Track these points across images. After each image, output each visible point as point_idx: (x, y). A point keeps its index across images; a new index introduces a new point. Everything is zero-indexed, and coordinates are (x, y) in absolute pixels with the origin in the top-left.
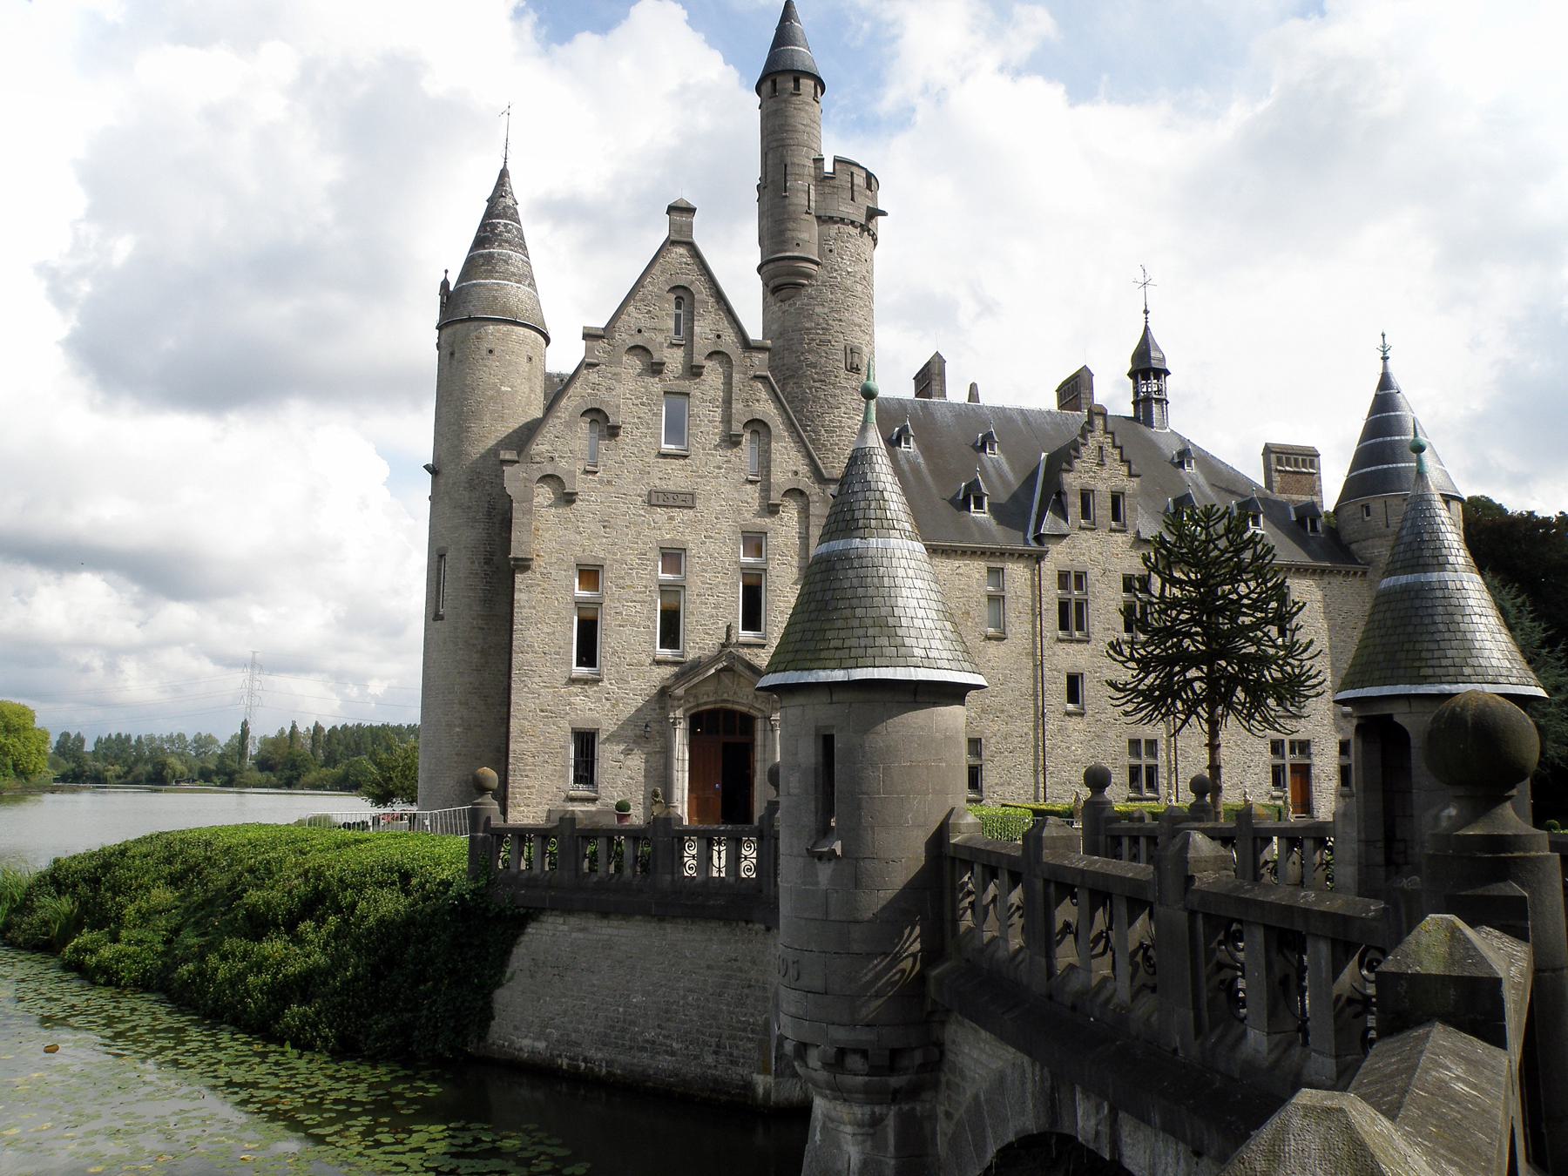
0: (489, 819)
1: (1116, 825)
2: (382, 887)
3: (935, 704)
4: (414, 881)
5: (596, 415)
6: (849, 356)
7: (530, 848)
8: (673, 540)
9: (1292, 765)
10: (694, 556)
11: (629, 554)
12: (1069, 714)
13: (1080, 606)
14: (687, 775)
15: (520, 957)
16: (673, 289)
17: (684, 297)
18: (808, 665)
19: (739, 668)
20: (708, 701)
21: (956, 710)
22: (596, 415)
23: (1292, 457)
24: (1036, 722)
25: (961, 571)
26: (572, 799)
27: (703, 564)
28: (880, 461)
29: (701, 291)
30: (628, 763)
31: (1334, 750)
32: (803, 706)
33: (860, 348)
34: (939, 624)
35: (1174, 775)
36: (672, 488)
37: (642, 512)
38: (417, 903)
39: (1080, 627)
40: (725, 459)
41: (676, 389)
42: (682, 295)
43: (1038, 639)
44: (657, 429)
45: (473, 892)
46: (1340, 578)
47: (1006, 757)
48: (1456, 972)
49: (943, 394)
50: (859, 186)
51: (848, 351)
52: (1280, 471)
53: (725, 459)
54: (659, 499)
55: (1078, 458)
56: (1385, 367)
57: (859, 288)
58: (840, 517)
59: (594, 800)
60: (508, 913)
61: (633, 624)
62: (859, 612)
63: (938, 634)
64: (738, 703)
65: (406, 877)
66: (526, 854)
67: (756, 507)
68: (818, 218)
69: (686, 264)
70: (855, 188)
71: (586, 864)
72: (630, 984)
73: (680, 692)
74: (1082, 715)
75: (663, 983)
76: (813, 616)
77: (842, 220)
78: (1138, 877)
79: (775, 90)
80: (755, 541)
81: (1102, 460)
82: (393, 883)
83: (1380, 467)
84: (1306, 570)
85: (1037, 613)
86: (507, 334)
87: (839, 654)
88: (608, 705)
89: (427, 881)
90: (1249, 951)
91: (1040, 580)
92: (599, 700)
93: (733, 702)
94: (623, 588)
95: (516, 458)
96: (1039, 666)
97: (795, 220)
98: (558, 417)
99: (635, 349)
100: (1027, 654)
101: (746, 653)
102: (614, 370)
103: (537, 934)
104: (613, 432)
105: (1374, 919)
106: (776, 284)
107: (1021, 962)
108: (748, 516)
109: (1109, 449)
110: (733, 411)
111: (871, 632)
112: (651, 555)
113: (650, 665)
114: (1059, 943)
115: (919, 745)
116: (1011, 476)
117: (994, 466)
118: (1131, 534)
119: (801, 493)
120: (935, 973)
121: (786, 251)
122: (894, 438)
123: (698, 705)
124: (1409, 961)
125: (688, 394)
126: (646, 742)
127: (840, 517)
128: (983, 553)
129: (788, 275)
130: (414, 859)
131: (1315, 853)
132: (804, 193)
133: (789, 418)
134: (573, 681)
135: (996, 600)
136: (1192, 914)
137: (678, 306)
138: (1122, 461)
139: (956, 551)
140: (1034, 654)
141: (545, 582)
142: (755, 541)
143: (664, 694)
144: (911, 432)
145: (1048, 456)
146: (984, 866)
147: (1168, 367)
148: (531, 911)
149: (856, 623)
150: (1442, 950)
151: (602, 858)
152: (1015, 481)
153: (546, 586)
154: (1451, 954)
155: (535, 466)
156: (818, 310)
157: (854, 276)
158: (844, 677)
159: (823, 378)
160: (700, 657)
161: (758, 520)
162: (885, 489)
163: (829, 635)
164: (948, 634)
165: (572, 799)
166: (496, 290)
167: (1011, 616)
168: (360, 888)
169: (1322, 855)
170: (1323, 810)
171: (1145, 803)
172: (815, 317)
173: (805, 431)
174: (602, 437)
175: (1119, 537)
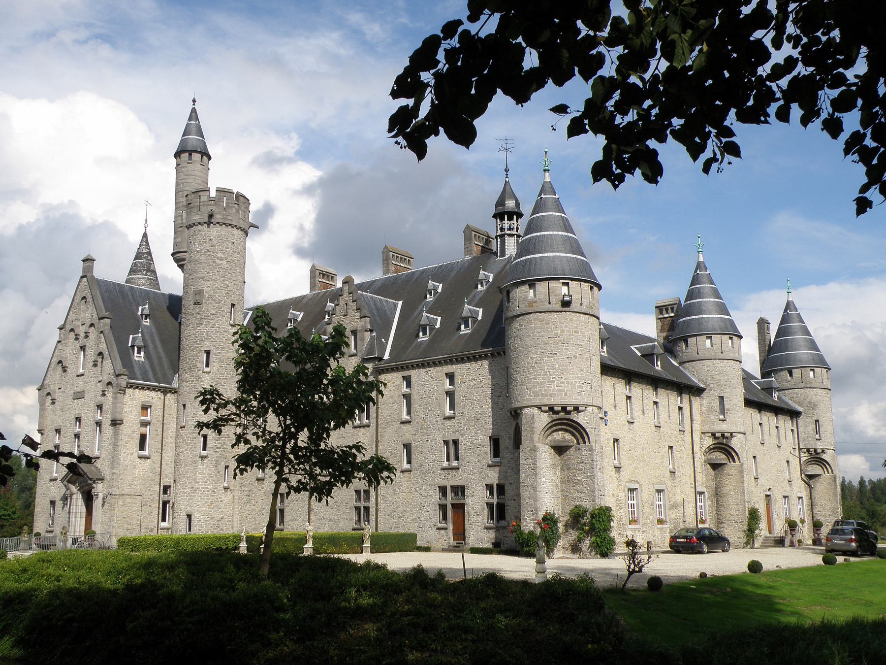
47: (295, 504)
59: (52, 532)
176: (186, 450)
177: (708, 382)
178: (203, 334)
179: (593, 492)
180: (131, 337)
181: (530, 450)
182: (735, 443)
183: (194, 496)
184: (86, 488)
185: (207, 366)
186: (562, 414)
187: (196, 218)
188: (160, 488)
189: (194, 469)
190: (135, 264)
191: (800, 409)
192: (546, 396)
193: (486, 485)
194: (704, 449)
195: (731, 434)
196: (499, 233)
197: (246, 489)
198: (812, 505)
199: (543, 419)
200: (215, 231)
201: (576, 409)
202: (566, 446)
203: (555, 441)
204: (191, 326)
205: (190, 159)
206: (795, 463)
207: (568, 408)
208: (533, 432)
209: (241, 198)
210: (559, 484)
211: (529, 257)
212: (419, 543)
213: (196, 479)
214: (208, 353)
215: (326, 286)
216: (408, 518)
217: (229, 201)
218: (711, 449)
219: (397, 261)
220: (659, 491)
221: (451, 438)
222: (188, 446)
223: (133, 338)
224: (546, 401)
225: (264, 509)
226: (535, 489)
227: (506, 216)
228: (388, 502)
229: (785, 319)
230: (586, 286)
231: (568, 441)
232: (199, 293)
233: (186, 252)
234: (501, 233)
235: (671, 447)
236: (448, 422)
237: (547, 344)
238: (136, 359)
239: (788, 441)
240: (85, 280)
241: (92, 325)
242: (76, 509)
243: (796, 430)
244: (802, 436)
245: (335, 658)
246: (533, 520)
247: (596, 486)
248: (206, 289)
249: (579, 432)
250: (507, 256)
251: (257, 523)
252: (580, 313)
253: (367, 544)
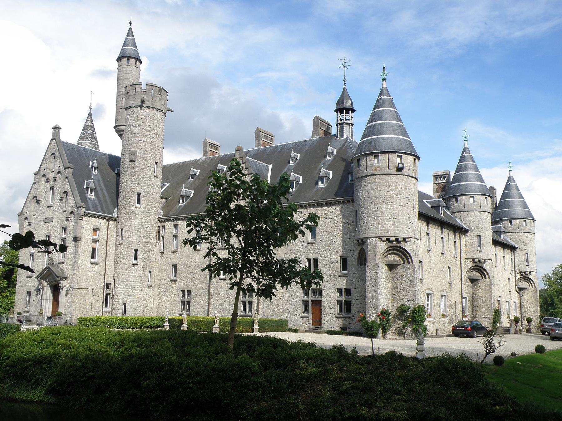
9: (312, 301)
59: (28, 312)
102: (39, 183)
157: (135, 126)
176: (123, 260)
177: (471, 226)
178: (136, 182)
179: (414, 295)
180: (86, 181)
181: (373, 266)
182: (487, 266)
183: (128, 290)
184: (53, 283)
185: (138, 203)
186: (395, 243)
187: (132, 103)
188: (104, 284)
189: (129, 272)
190: (83, 133)
191: (516, 246)
192: (385, 230)
193: (337, 289)
194: (467, 269)
195: (485, 260)
196: (339, 122)
197: (163, 287)
198: (521, 307)
199: (382, 246)
200: (145, 112)
201: (405, 240)
202: (396, 265)
203: (388, 261)
204: (128, 176)
205: (128, 62)
206: (513, 280)
207: (400, 239)
208: (376, 255)
209: (163, 91)
210: (390, 290)
211: (374, 137)
212: (289, 326)
213: (129, 279)
214: (139, 194)
215: (213, 153)
216: (280, 309)
217: (155, 93)
218: (471, 270)
219: (264, 139)
220: (443, 296)
221: (312, 257)
222: (124, 256)
223: (87, 182)
224: (385, 234)
225: (175, 300)
226: (376, 293)
227: (344, 111)
229: (507, 187)
230: (412, 158)
231: (397, 261)
232: (134, 153)
233: (125, 125)
234: (341, 122)
235: (449, 268)
236: (310, 246)
237: (386, 196)
238: (90, 197)
239: (509, 266)
240: (54, 141)
241: (59, 172)
242: (46, 297)
243: (513, 259)
244: (517, 263)
245: (304, 411)
246: (375, 313)
247: (416, 292)
248: (138, 151)
249: (405, 255)
250: (344, 138)
251: (170, 309)
252: (408, 176)
253: (256, 326)
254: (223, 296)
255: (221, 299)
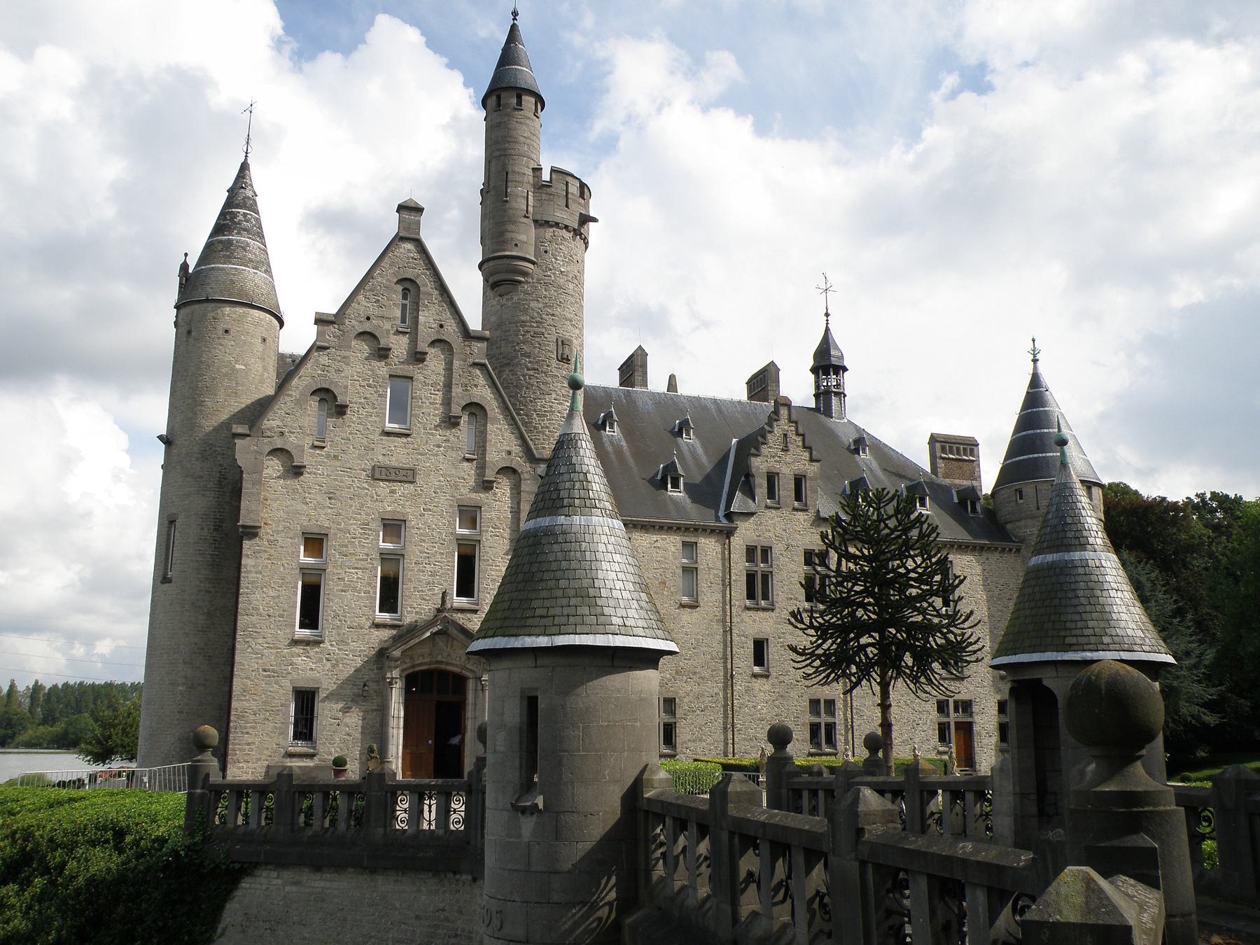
0: (207, 775)
1: (797, 780)
2: (94, 846)
3: (631, 669)
4: (128, 839)
5: (325, 395)
6: (560, 348)
7: (247, 803)
8: (394, 512)
9: (957, 723)
10: (413, 527)
11: (352, 524)
12: (755, 676)
13: (766, 577)
14: (401, 731)
15: (232, 912)
16: (400, 281)
17: (410, 288)
18: (515, 631)
19: (453, 631)
20: (423, 661)
21: (650, 673)
22: (325, 395)
23: (955, 446)
24: (725, 683)
25: (658, 544)
26: (291, 755)
27: (421, 535)
28: (584, 446)
29: (427, 284)
30: (347, 720)
31: (994, 710)
32: (510, 669)
33: (571, 341)
34: (635, 595)
35: (850, 732)
36: (395, 464)
37: (365, 485)
38: (130, 861)
39: (765, 597)
40: (445, 438)
41: (401, 373)
42: (409, 286)
43: (728, 607)
44: (382, 409)
45: (188, 848)
46: (997, 555)
47: (698, 715)
48: (1092, 920)
49: (645, 384)
50: (572, 194)
51: (560, 343)
52: (944, 458)
53: (445, 438)
54: (381, 474)
55: (765, 444)
56: (1035, 368)
57: (571, 286)
58: (547, 496)
59: (311, 756)
60: (223, 867)
61: (355, 589)
62: (563, 583)
63: (635, 604)
64: (452, 664)
65: (120, 834)
66: (243, 809)
67: (472, 483)
68: (536, 222)
69: (413, 258)
70: (569, 196)
71: (302, 818)
72: (340, 936)
73: (397, 653)
74: (767, 677)
75: (373, 934)
76: (521, 586)
77: (557, 225)
78: (814, 830)
79: (499, 104)
80: (470, 515)
81: (787, 447)
82: (107, 841)
83: (1031, 456)
84: (967, 547)
85: (726, 584)
86: (244, 315)
87: (544, 621)
88: (328, 665)
89: (141, 838)
90: (915, 898)
91: (730, 554)
92: (320, 660)
93: (447, 664)
94: (346, 556)
95: (248, 432)
96: (728, 632)
97: (514, 223)
98: (289, 395)
99: (362, 335)
100: (717, 621)
101: (458, 617)
102: (344, 353)
103: (250, 888)
104: (341, 410)
105: (1024, 868)
106: (495, 279)
107: (708, 910)
108: (464, 491)
109: (792, 436)
110: (453, 394)
111: (573, 601)
112: (373, 526)
113: (370, 627)
114: (743, 891)
115: (616, 706)
116: (704, 459)
117: (690, 450)
118: (811, 514)
119: (514, 471)
120: (629, 921)
121: (505, 250)
122: (600, 422)
123: (414, 666)
124: (1050, 910)
125: (412, 378)
126: (363, 701)
127: (547, 496)
128: (679, 528)
129: (507, 272)
130: (129, 817)
131: (975, 805)
132: (522, 198)
133: (504, 402)
134: (295, 642)
135: (690, 571)
136: (863, 863)
137: (405, 297)
138: (804, 447)
139: (654, 527)
140: (724, 621)
141: (271, 548)
142: (470, 515)
143: (382, 655)
144: (615, 417)
145: (738, 442)
146: (675, 819)
147: (846, 363)
148: (246, 866)
149: (560, 593)
150: (1079, 900)
151: (318, 812)
152: (707, 464)
153: (272, 552)
154: (1087, 903)
155: (266, 440)
156: (533, 304)
158: (548, 643)
159: (536, 367)
160: (416, 621)
161: (474, 495)
162: (588, 472)
163: (535, 604)
164: (644, 604)
165: (291, 755)
166: (234, 275)
167: (703, 586)
168: (70, 848)
169: (981, 806)
170: (984, 764)
171: (824, 758)
172: (530, 311)
173: (519, 414)
174: (330, 415)
175: (801, 516)
184: (442, 666)
227: (831, 369)
228: (865, 717)
254: (764, 711)
255: (759, 720)
